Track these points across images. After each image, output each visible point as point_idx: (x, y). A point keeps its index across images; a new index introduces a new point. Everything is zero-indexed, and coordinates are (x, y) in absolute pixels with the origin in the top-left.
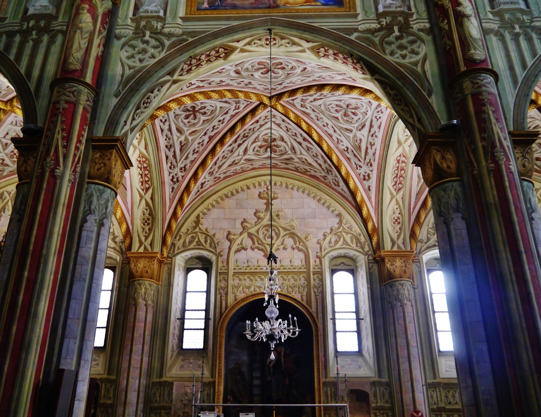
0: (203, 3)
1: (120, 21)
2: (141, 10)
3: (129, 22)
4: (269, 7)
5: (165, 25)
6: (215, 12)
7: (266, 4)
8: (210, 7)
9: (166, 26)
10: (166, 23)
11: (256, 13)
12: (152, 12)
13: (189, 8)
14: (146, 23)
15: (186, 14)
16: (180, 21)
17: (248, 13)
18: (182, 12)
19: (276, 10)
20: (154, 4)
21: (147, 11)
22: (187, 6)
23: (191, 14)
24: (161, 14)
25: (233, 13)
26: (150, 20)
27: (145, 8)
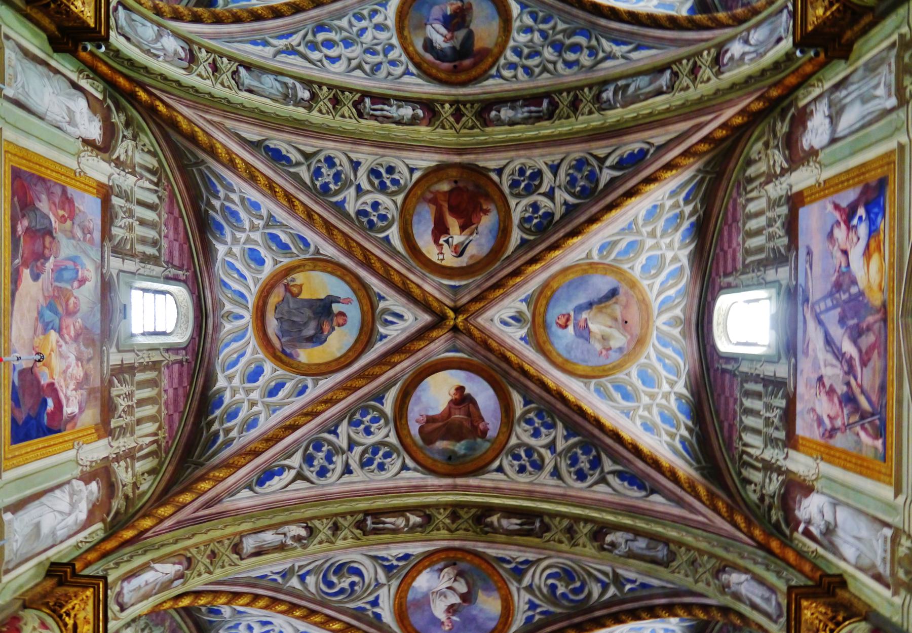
0: (876, 449)
1: (896, 619)
2: (881, 569)
3: (898, 600)
4: (885, 320)
5: (904, 531)
6: (889, 428)
7: (880, 328)
8: (881, 436)
9: (906, 529)
10: (901, 526)
11: (892, 348)
12: (885, 551)
13: (882, 477)
14: (902, 567)
15: (890, 484)
16: (901, 499)
17: (893, 363)
18: (887, 492)
19: (890, 308)
20: (874, 542)
21: (884, 559)
22: (879, 480)
23: (890, 476)
24: (888, 532)
25: (892, 390)
26: (896, 558)
27: (879, 562)
